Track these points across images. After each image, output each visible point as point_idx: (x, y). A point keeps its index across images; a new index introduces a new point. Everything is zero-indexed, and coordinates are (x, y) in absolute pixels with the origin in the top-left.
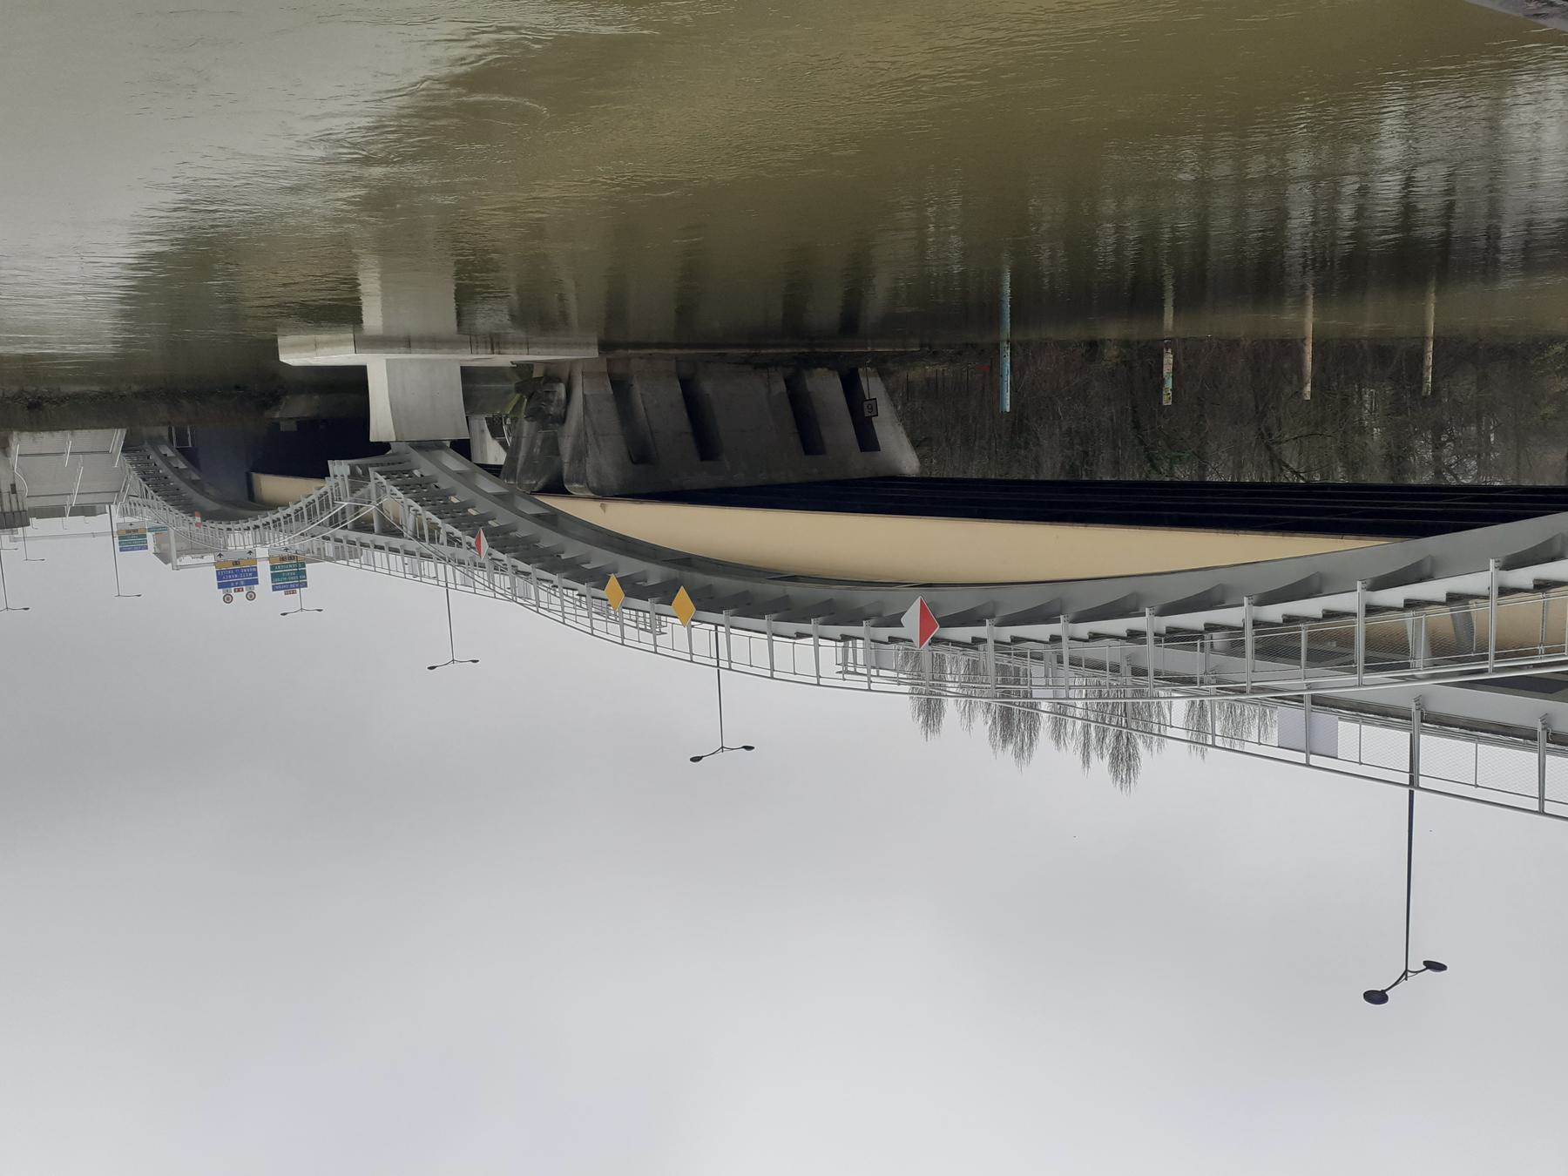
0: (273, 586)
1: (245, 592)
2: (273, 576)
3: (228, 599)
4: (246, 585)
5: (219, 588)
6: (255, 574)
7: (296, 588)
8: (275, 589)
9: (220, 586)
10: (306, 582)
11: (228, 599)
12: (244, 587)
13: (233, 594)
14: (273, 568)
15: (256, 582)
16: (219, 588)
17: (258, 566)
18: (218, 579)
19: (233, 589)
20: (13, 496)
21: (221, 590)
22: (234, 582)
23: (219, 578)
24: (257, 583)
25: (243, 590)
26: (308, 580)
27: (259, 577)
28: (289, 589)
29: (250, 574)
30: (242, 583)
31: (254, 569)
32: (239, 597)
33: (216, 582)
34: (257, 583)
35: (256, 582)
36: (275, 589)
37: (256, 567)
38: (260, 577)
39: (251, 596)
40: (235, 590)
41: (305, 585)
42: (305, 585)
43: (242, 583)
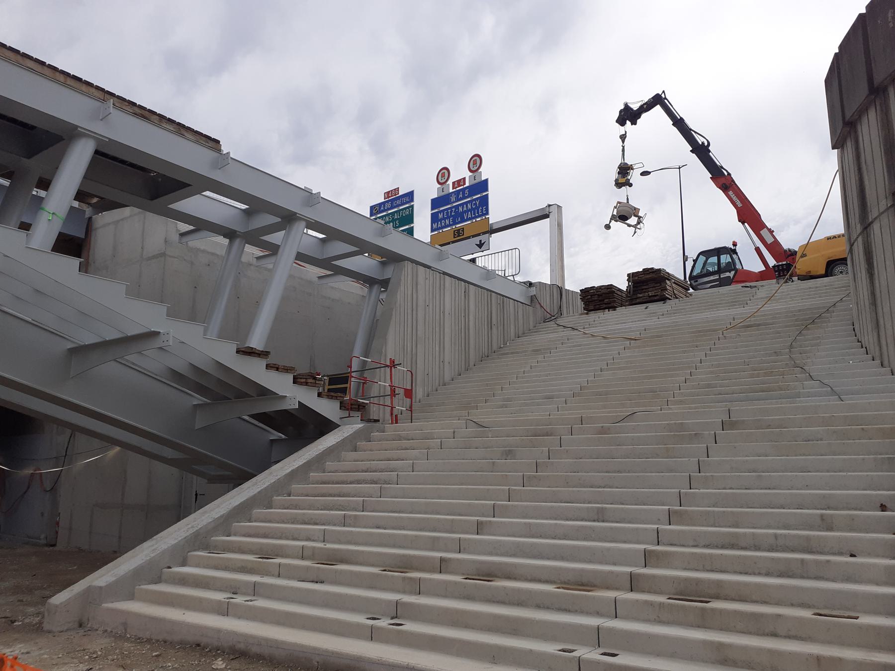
0: (412, 200)
1: (450, 182)
3: (476, 162)
4: (450, 194)
9: (483, 186)
11: (476, 162)
12: (451, 190)
13: (467, 174)
17: (429, 234)
19: (467, 184)
21: (483, 179)
23: (485, 201)
30: (453, 199)
32: (460, 172)
35: (435, 203)
37: (432, 230)
40: (464, 184)
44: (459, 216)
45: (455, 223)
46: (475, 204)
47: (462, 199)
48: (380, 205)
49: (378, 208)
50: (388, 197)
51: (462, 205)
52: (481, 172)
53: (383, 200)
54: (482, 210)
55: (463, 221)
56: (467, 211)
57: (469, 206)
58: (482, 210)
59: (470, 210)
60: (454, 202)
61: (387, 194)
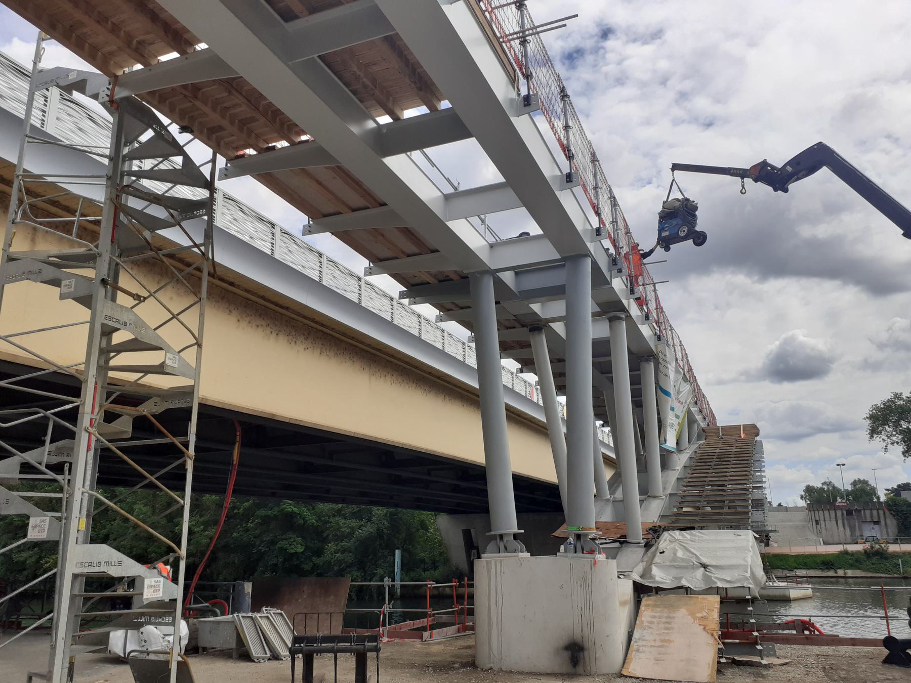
20: (817, 519)
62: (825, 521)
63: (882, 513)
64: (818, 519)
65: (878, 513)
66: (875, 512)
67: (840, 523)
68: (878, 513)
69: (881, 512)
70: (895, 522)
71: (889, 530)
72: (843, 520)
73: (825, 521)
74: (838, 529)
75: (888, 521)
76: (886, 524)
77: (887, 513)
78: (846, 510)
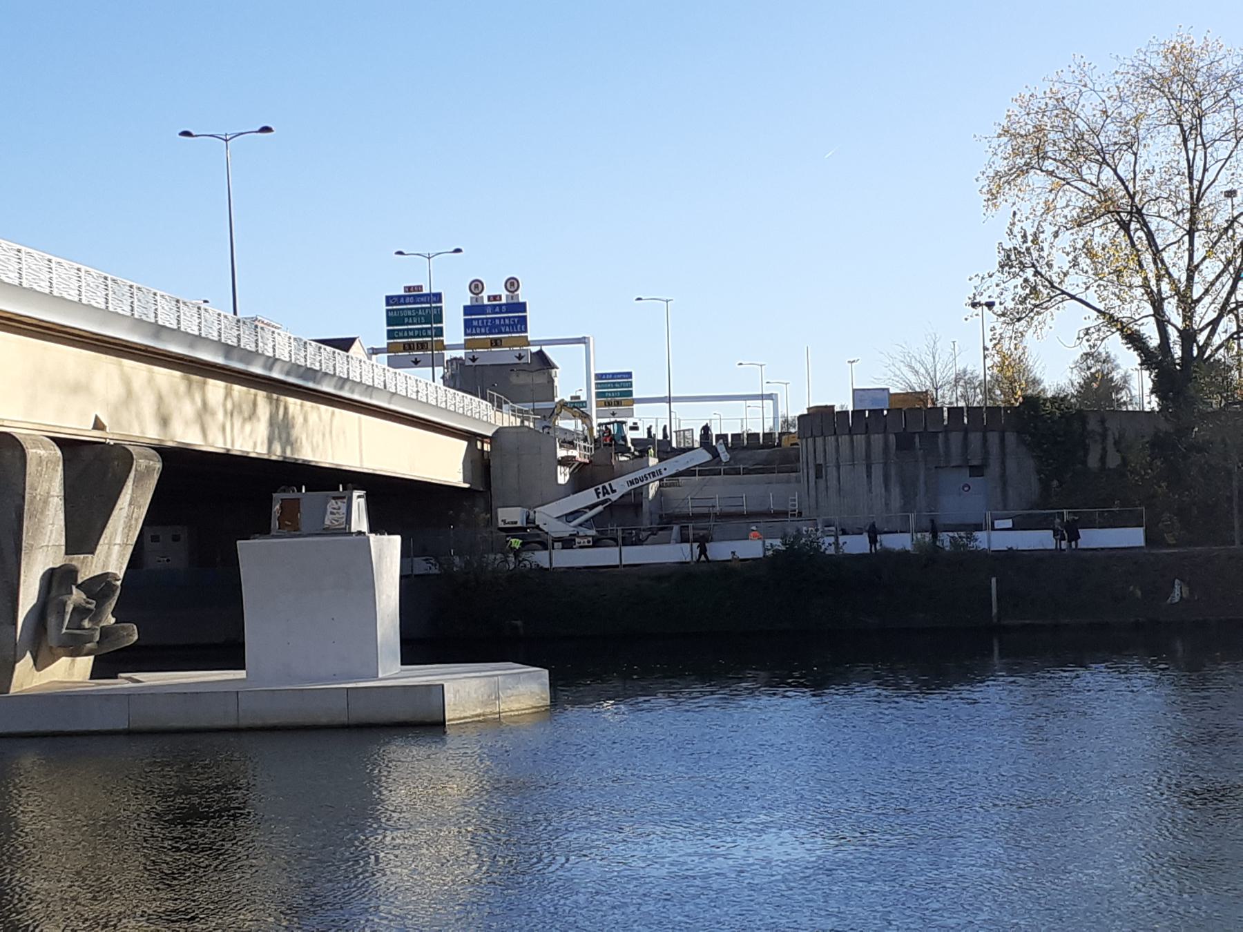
1: (485, 295)
2: (439, 319)
3: (512, 284)
5: (524, 304)
6: (468, 324)
7: (404, 297)
8: (438, 297)
9: (522, 307)
10: (388, 304)
11: (512, 284)
12: (486, 302)
14: (440, 332)
15: (468, 311)
16: (524, 304)
18: (525, 317)
19: (504, 301)
20: (820, 461)
21: (521, 300)
22: (501, 312)
23: (523, 320)
24: (466, 308)
25: (489, 298)
26: (384, 308)
27: (462, 318)
28: (414, 294)
29: (475, 323)
31: (469, 331)
32: (494, 287)
33: (528, 314)
34: (466, 308)
35: (468, 311)
36: (438, 297)
37: (466, 334)
38: (461, 318)
39: (476, 286)
40: (501, 299)
41: (390, 300)
42: (390, 300)
43: (489, 310)
44: (493, 327)
45: (491, 333)
46: (514, 321)
47: (497, 313)
48: (399, 297)
49: (396, 299)
50: (409, 291)
51: (500, 318)
52: (518, 295)
53: (402, 292)
54: (521, 328)
55: (500, 332)
56: (505, 325)
57: (507, 321)
58: (521, 328)
59: (509, 325)
60: (489, 314)
61: (408, 289)
62: (838, 467)
63: (997, 441)
64: (822, 462)
65: (985, 440)
66: (975, 438)
67: (877, 471)
68: (985, 440)
69: (993, 438)
70: (1030, 463)
71: (1011, 492)
72: (885, 464)
73: (838, 467)
74: (870, 490)
75: (1011, 464)
76: (1003, 475)
77: (1011, 437)
78: (895, 434)
